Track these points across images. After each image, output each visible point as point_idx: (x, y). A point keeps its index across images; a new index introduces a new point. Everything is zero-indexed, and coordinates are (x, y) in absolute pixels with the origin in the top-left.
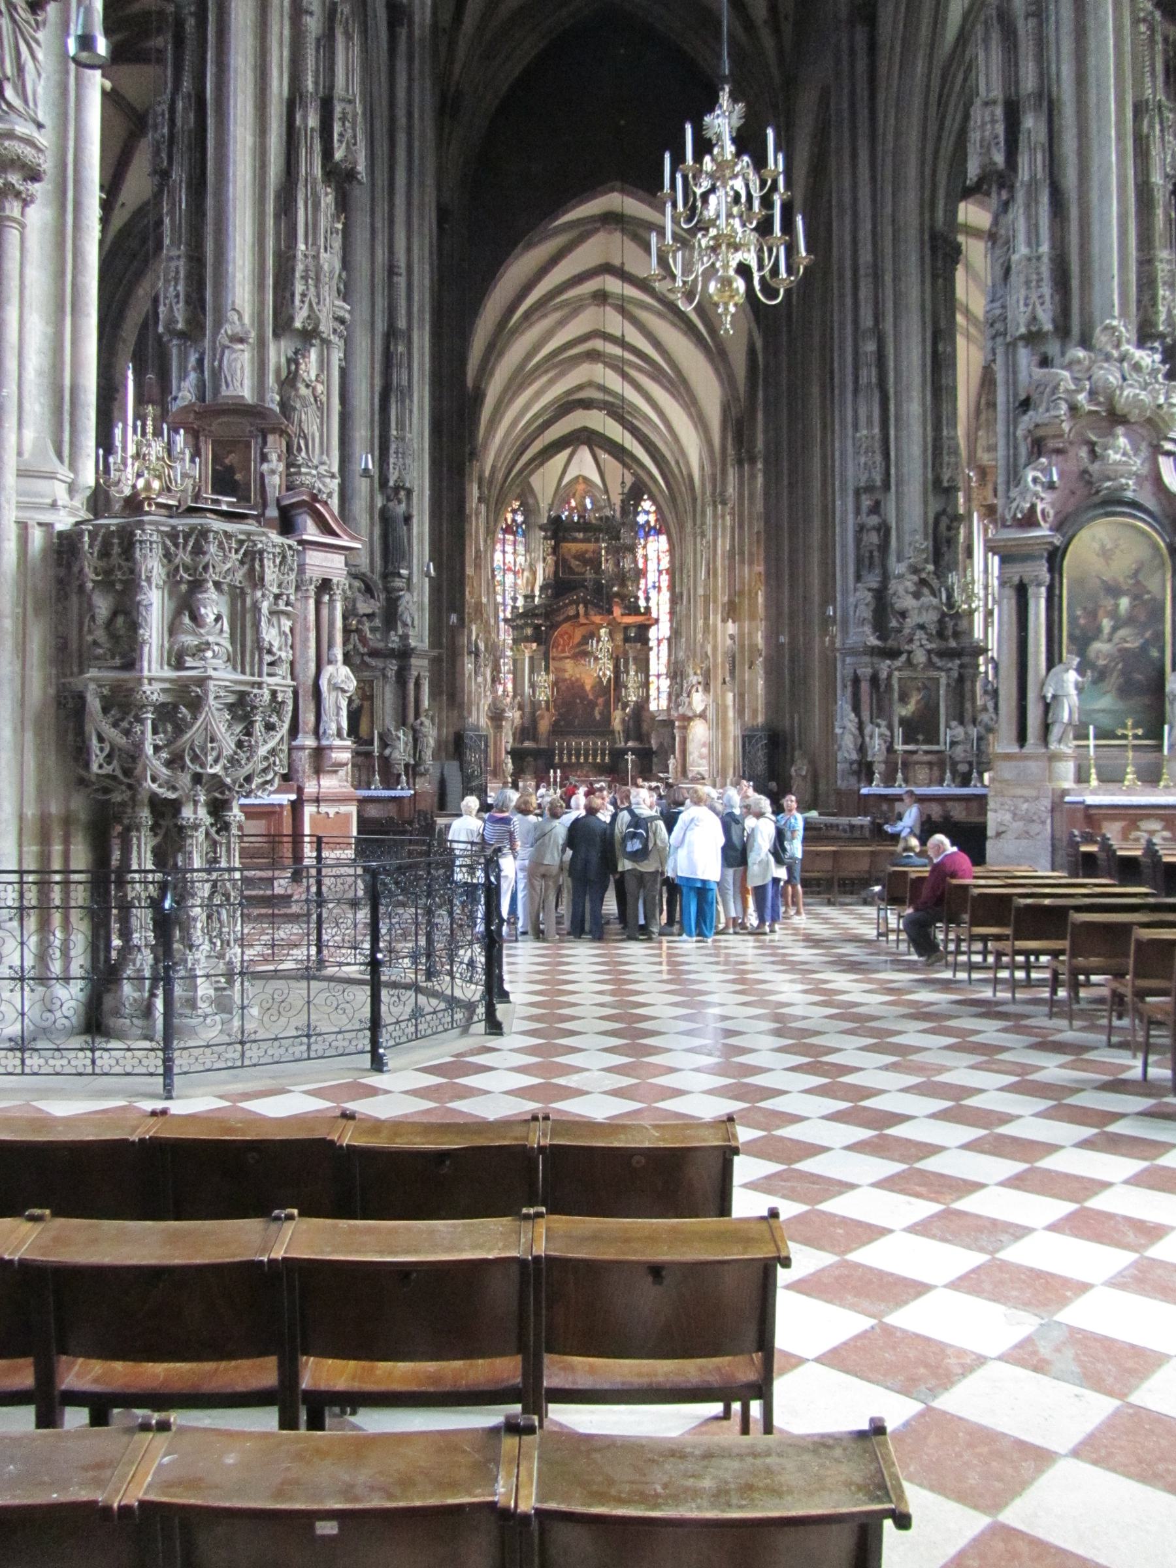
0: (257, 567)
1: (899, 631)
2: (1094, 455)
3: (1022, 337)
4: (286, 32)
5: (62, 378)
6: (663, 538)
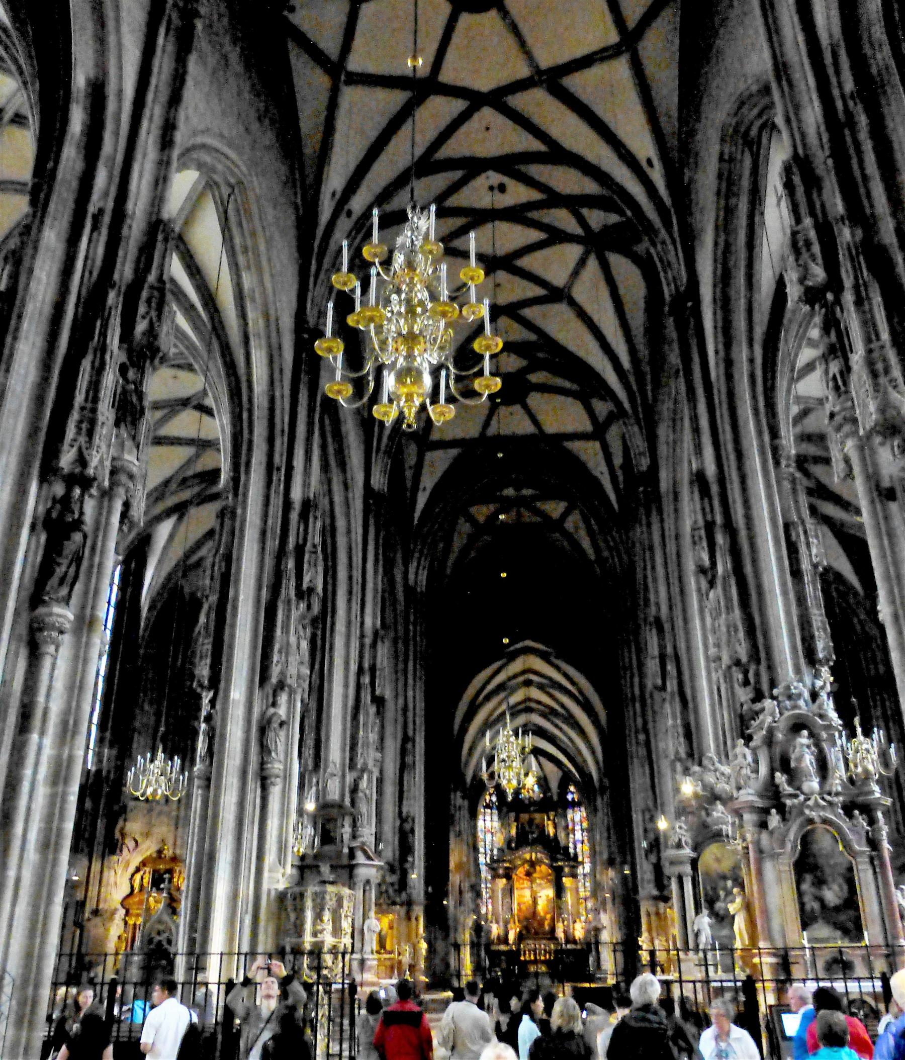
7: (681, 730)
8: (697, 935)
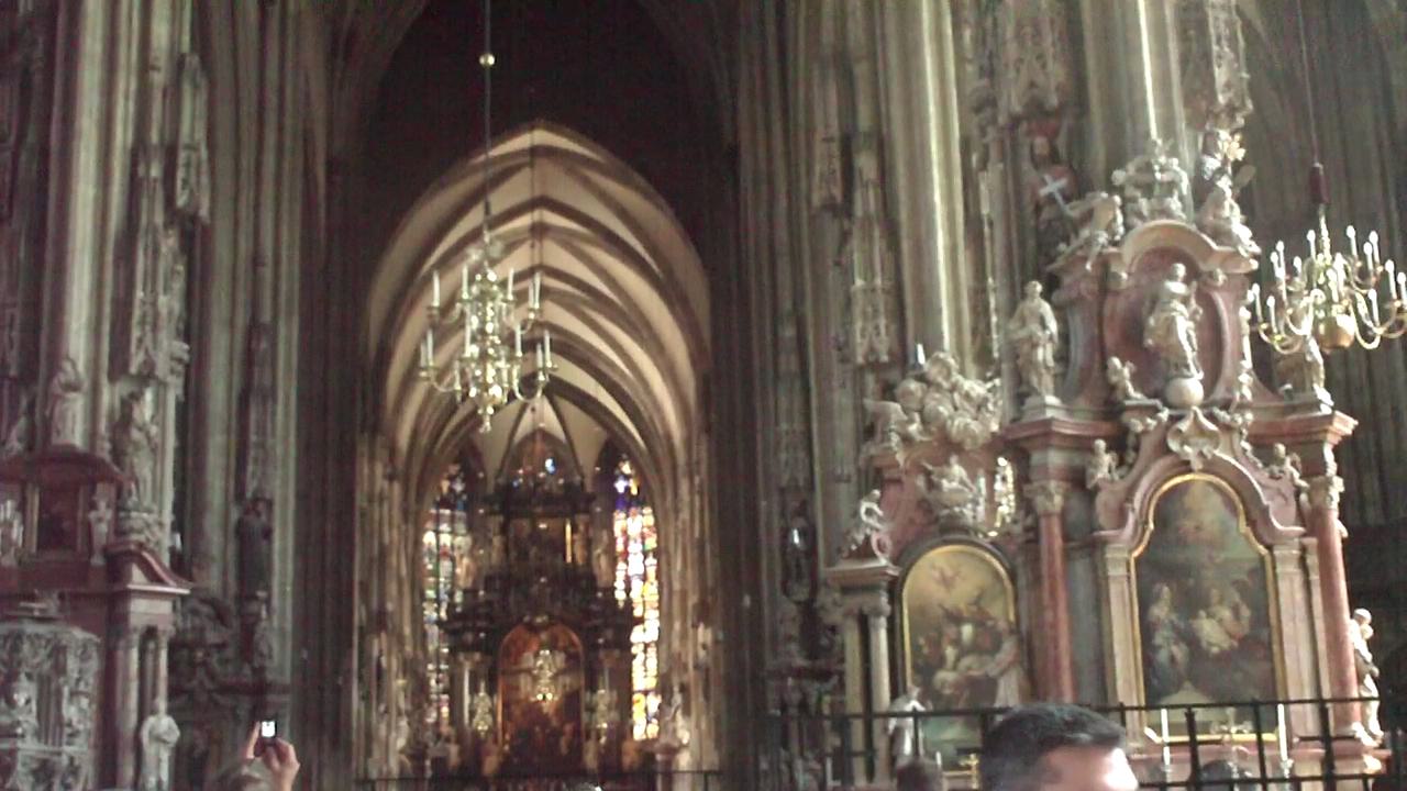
4: (133, 86)
6: (647, 510)
7: (881, 301)
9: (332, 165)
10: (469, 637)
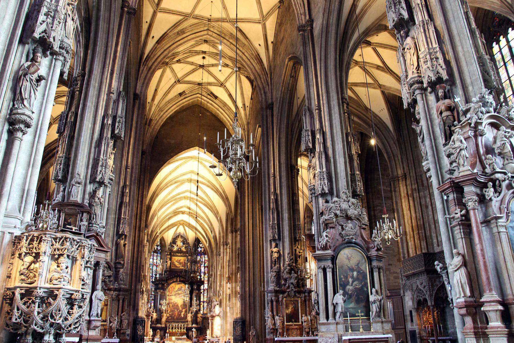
0: (83, 251)
1: (285, 285)
2: (343, 229)
3: (320, 194)
5: (25, 186)
6: (206, 256)
8: (335, 306)
9: (143, 153)
10: (160, 286)
